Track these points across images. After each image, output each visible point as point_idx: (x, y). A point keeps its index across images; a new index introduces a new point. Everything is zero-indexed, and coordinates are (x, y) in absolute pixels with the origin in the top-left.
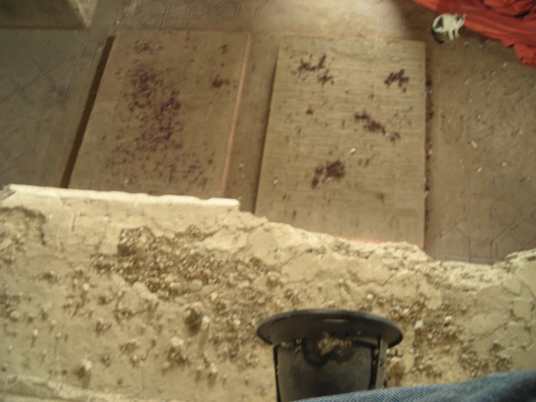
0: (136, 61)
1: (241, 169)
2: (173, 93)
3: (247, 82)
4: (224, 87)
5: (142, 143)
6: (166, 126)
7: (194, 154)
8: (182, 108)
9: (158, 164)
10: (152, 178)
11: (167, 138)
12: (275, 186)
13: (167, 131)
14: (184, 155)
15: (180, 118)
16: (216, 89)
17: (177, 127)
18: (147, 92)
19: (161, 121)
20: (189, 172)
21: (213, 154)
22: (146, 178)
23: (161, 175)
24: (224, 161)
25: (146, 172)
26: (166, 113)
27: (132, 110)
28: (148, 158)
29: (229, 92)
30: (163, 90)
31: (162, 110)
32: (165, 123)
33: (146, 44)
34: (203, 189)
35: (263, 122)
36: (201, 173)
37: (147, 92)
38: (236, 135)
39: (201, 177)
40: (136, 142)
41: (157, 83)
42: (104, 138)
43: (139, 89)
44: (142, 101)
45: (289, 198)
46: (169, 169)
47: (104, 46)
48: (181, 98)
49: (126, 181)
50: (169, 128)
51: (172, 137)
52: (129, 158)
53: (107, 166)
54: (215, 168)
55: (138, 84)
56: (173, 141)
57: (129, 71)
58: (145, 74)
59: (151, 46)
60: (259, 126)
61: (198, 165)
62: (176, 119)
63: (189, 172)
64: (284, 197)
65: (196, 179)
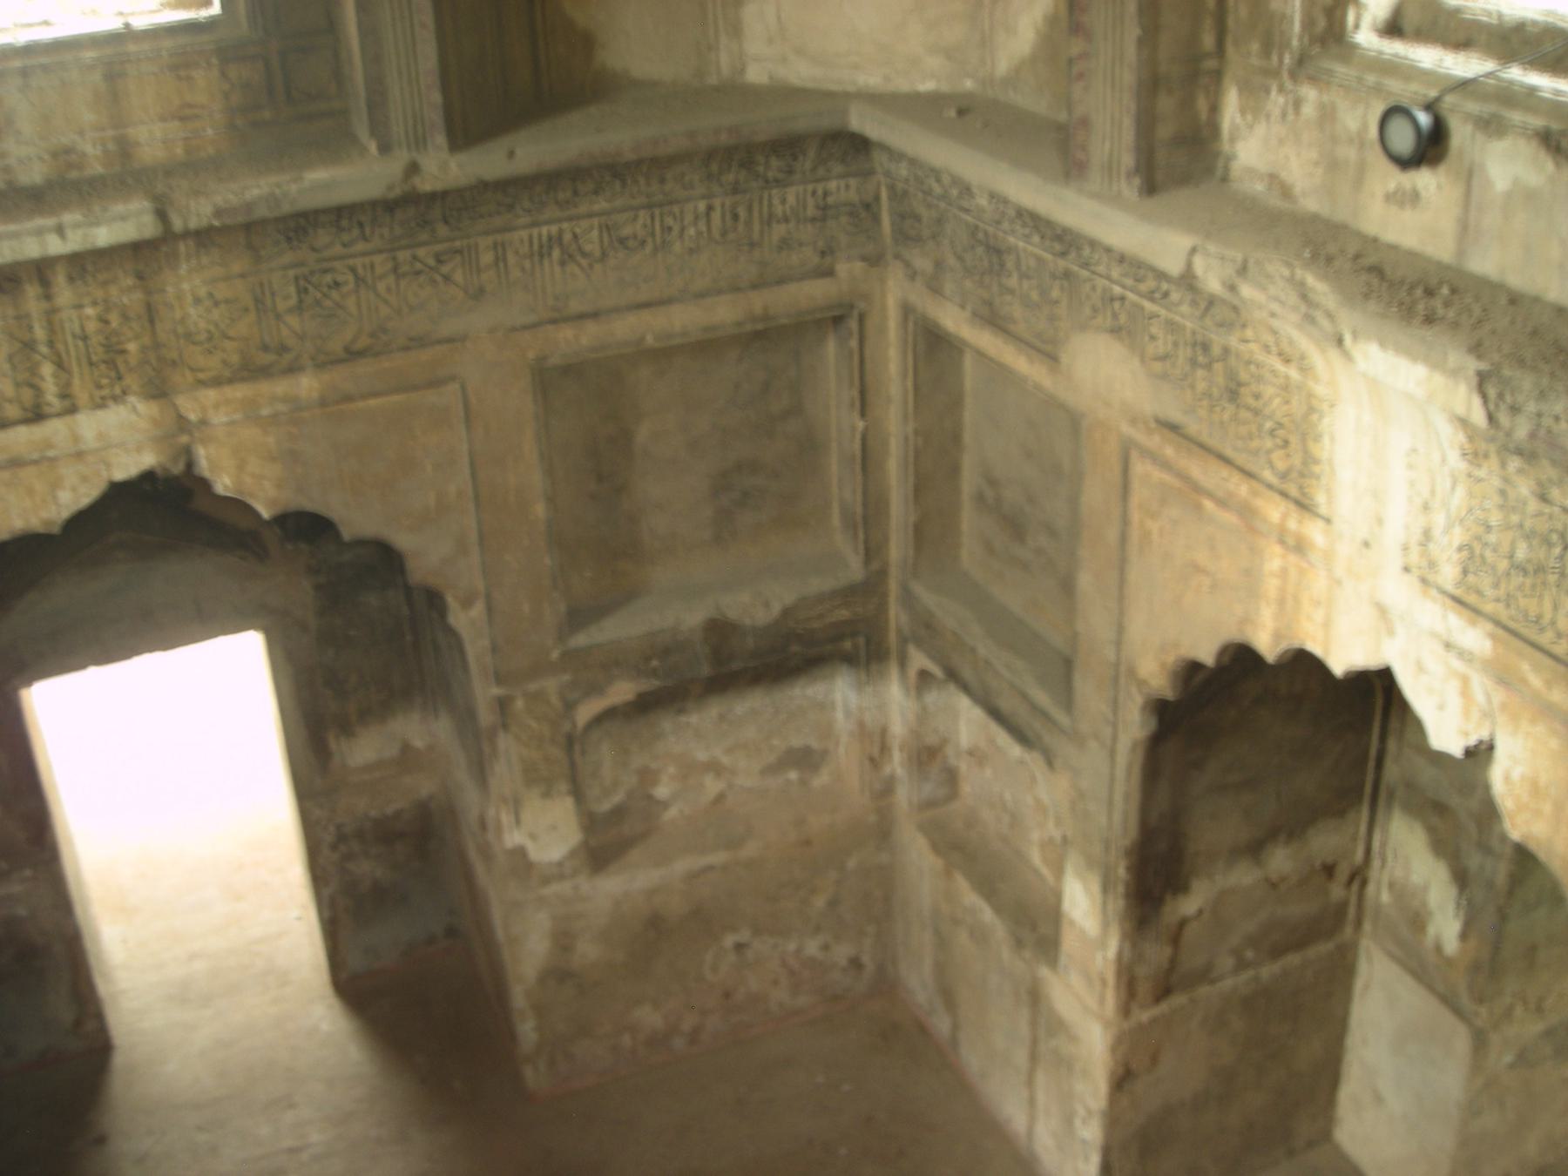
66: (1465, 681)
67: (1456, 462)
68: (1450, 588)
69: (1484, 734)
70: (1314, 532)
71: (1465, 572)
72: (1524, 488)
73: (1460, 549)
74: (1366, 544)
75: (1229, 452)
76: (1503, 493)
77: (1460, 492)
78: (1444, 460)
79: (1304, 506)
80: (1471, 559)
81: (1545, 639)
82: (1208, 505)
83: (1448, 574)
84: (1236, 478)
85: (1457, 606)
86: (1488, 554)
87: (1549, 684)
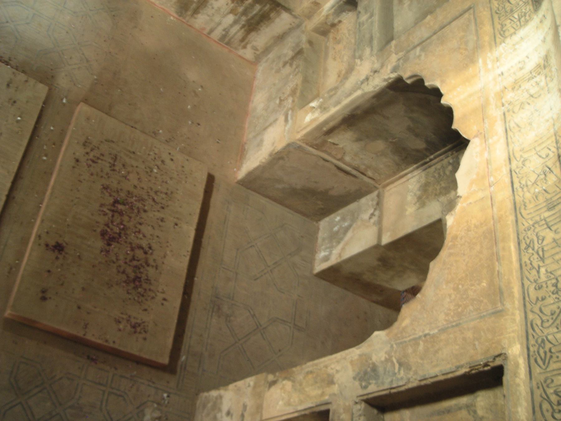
0: (146, 310)
1: (46, 156)
2: (108, 252)
3: (25, 241)
4: (52, 243)
5: (139, 205)
6: (116, 215)
7: (92, 174)
8: (99, 230)
9: (125, 177)
10: (132, 166)
11: (116, 202)
12: (20, 117)
13: (115, 209)
14: (102, 177)
15: (102, 220)
16: (60, 241)
17: (105, 209)
18: (135, 263)
19: (121, 223)
20: (98, 158)
21: (74, 167)
22: (137, 167)
23: (124, 165)
24: (63, 157)
25: (138, 173)
26: (117, 230)
27: (150, 248)
28: (135, 187)
29: (47, 233)
30: (117, 260)
31: (119, 235)
32: (117, 219)
33: (135, 332)
34: (88, 139)
35: (14, 198)
36: (87, 153)
37: (135, 263)
38: (44, 193)
39: (88, 150)
40: (146, 208)
41: (124, 272)
42: (176, 224)
43: (142, 270)
44: (139, 253)
45: (10, 99)
46: (117, 168)
47: (179, 363)
48: (100, 244)
49: (155, 171)
50: (113, 211)
51: (111, 200)
52: (152, 194)
53: (172, 193)
54: (74, 154)
55: (144, 277)
56: (111, 196)
57: (153, 298)
58: (136, 288)
59: (129, 328)
60: (19, 195)
61: (90, 162)
62: (106, 218)
63: (98, 158)
64: (15, 102)
65: (92, 150)
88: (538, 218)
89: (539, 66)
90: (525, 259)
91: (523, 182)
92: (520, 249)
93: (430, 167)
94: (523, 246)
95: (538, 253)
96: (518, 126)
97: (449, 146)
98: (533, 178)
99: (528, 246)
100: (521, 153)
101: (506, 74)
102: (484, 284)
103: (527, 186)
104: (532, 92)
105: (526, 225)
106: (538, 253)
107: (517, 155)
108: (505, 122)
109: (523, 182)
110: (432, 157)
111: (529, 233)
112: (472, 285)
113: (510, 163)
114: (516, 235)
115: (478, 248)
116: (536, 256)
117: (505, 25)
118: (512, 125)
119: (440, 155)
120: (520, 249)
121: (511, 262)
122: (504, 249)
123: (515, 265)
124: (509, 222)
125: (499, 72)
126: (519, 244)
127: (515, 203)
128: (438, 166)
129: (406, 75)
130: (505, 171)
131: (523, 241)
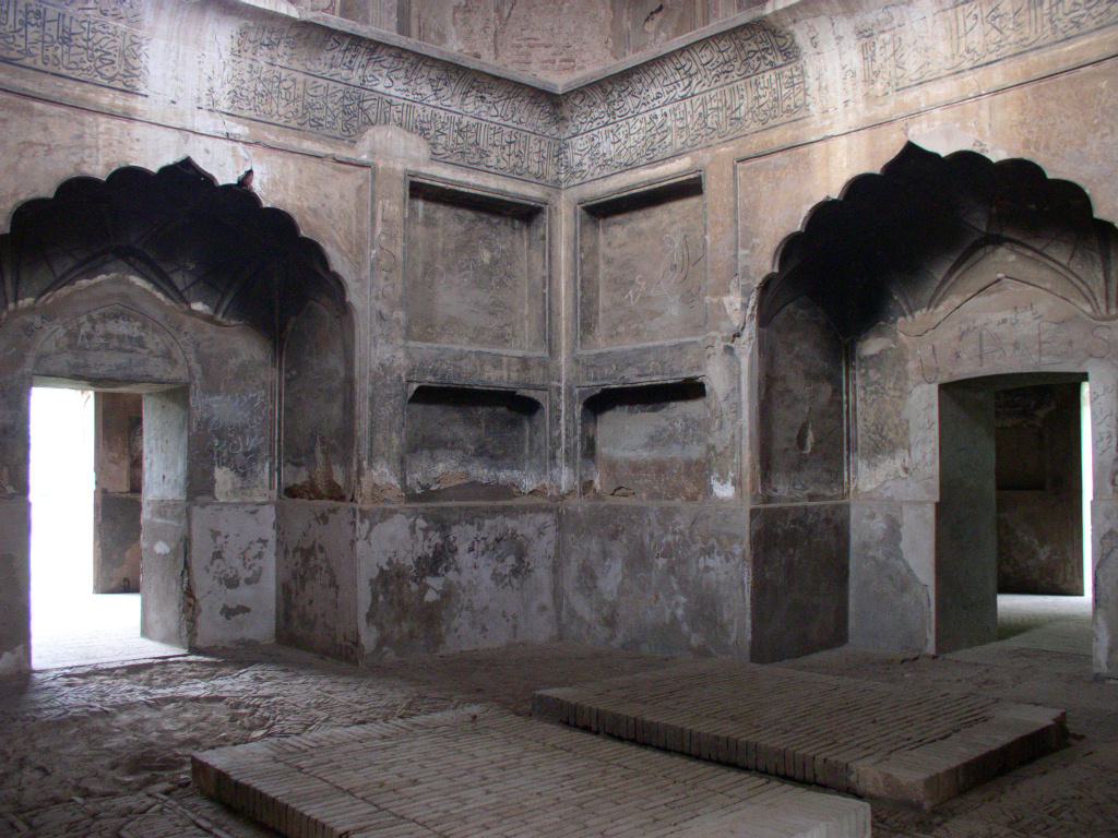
66: (234, 149)
67: (226, 56)
68: (226, 111)
69: (248, 169)
70: (137, 104)
71: (233, 102)
72: (262, 62)
73: (229, 93)
74: (174, 102)
75: (64, 71)
76: (251, 66)
77: (228, 69)
78: (221, 56)
79: (130, 91)
80: (235, 96)
81: (273, 120)
82: (38, 106)
83: (224, 105)
84: (70, 84)
85: (230, 117)
86: (244, 93)
87: (277, 137)
88: (1045, 18)
89: (863, 48)
90: (1091, 24)
91: (993, 47)
92: (1078, 35)
93: (855, 409)
94: (1075, 31)
95: (1089, 9)
96: (921, 68)
97: (844, 364)
98: (994, 34)
99: (1077, 24)
100: (956, 57)
101: (849, 97)
102: (1103, 85)
103: (1000, 41)
104: (889, 50)
105: (1049, 32)
106: (1089, 9)
107: (957, 61)
108: (909, 87)
109: (993, 47)
110: (845, 397)
111: (1061, 25)
112: (1099, 103)
113: (963, 71)
114: (1057, 46)
115: (1052, 104)
116: (1093, 11)
117: (789, 106)
118: (918, 75)
119: (847, 385)
120: (1078, 35)
121: (1089, 45)
122: (1067, 60)
123: (1094, 38)
124: (1036, 59)
125: (840, 106)
126: (1069, 38)
127: (1016, 55)
128: (860, 393)
129: (764, 263)
130: (970, 78)
131: (1069, 32)
